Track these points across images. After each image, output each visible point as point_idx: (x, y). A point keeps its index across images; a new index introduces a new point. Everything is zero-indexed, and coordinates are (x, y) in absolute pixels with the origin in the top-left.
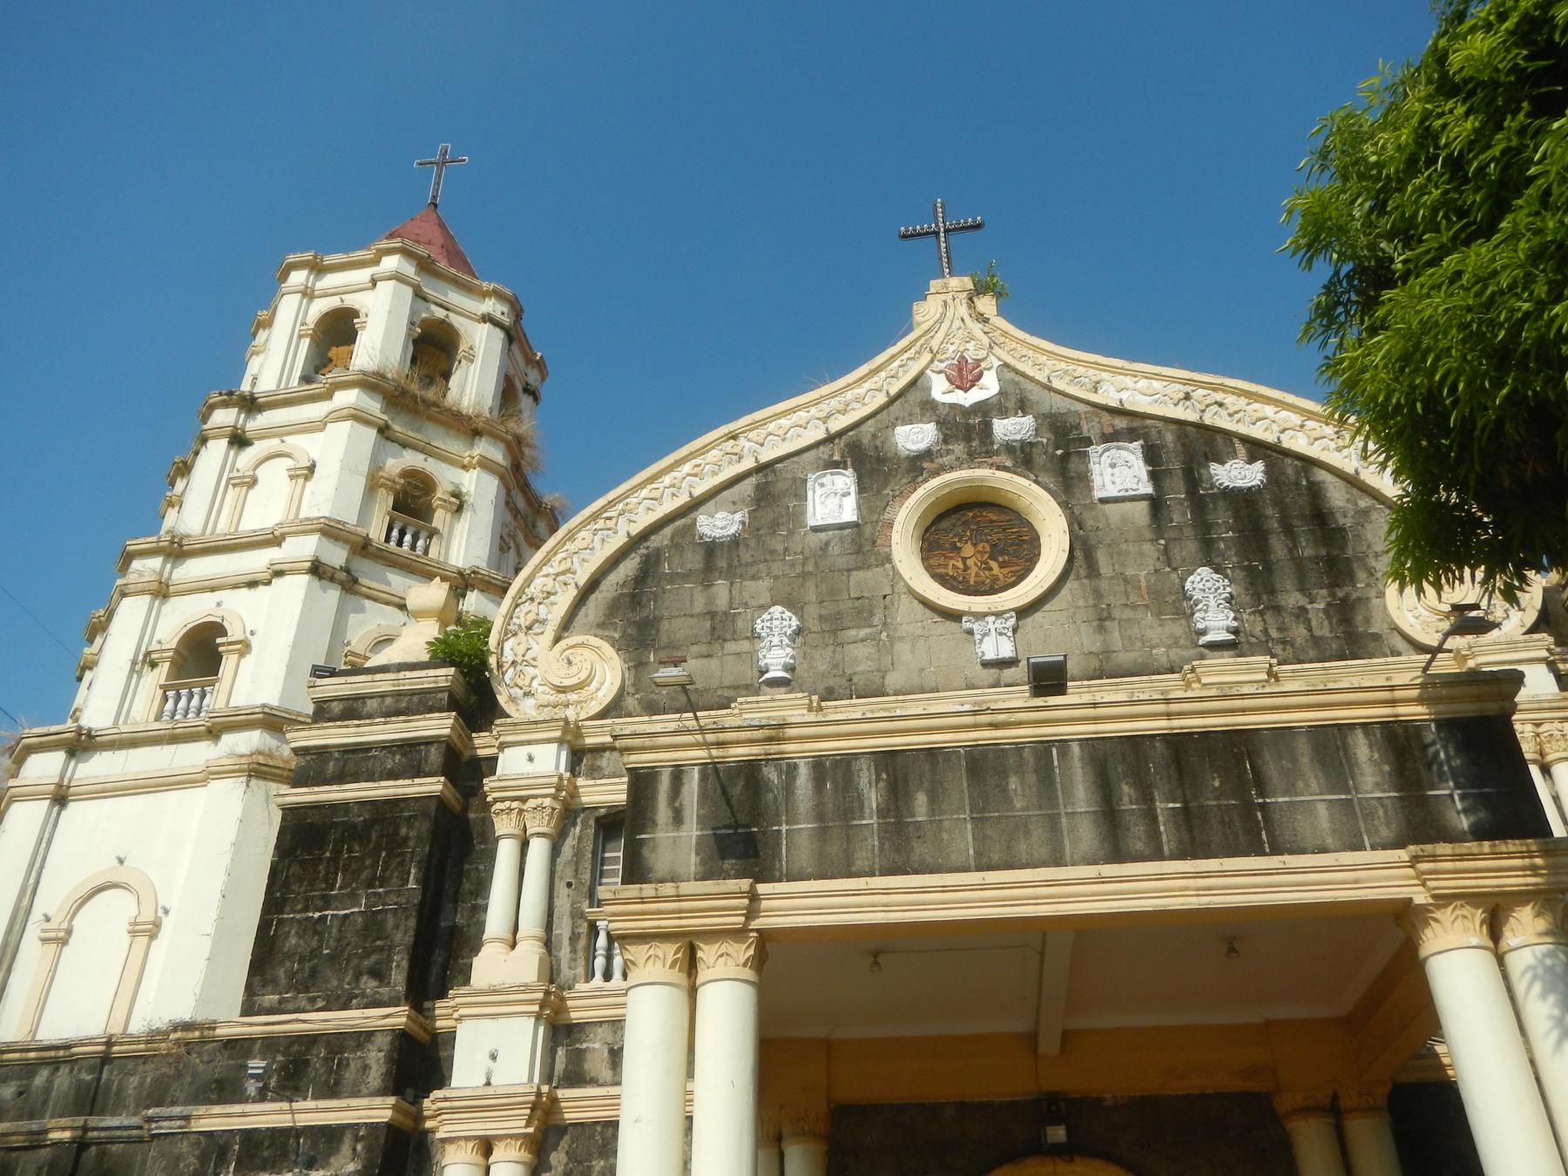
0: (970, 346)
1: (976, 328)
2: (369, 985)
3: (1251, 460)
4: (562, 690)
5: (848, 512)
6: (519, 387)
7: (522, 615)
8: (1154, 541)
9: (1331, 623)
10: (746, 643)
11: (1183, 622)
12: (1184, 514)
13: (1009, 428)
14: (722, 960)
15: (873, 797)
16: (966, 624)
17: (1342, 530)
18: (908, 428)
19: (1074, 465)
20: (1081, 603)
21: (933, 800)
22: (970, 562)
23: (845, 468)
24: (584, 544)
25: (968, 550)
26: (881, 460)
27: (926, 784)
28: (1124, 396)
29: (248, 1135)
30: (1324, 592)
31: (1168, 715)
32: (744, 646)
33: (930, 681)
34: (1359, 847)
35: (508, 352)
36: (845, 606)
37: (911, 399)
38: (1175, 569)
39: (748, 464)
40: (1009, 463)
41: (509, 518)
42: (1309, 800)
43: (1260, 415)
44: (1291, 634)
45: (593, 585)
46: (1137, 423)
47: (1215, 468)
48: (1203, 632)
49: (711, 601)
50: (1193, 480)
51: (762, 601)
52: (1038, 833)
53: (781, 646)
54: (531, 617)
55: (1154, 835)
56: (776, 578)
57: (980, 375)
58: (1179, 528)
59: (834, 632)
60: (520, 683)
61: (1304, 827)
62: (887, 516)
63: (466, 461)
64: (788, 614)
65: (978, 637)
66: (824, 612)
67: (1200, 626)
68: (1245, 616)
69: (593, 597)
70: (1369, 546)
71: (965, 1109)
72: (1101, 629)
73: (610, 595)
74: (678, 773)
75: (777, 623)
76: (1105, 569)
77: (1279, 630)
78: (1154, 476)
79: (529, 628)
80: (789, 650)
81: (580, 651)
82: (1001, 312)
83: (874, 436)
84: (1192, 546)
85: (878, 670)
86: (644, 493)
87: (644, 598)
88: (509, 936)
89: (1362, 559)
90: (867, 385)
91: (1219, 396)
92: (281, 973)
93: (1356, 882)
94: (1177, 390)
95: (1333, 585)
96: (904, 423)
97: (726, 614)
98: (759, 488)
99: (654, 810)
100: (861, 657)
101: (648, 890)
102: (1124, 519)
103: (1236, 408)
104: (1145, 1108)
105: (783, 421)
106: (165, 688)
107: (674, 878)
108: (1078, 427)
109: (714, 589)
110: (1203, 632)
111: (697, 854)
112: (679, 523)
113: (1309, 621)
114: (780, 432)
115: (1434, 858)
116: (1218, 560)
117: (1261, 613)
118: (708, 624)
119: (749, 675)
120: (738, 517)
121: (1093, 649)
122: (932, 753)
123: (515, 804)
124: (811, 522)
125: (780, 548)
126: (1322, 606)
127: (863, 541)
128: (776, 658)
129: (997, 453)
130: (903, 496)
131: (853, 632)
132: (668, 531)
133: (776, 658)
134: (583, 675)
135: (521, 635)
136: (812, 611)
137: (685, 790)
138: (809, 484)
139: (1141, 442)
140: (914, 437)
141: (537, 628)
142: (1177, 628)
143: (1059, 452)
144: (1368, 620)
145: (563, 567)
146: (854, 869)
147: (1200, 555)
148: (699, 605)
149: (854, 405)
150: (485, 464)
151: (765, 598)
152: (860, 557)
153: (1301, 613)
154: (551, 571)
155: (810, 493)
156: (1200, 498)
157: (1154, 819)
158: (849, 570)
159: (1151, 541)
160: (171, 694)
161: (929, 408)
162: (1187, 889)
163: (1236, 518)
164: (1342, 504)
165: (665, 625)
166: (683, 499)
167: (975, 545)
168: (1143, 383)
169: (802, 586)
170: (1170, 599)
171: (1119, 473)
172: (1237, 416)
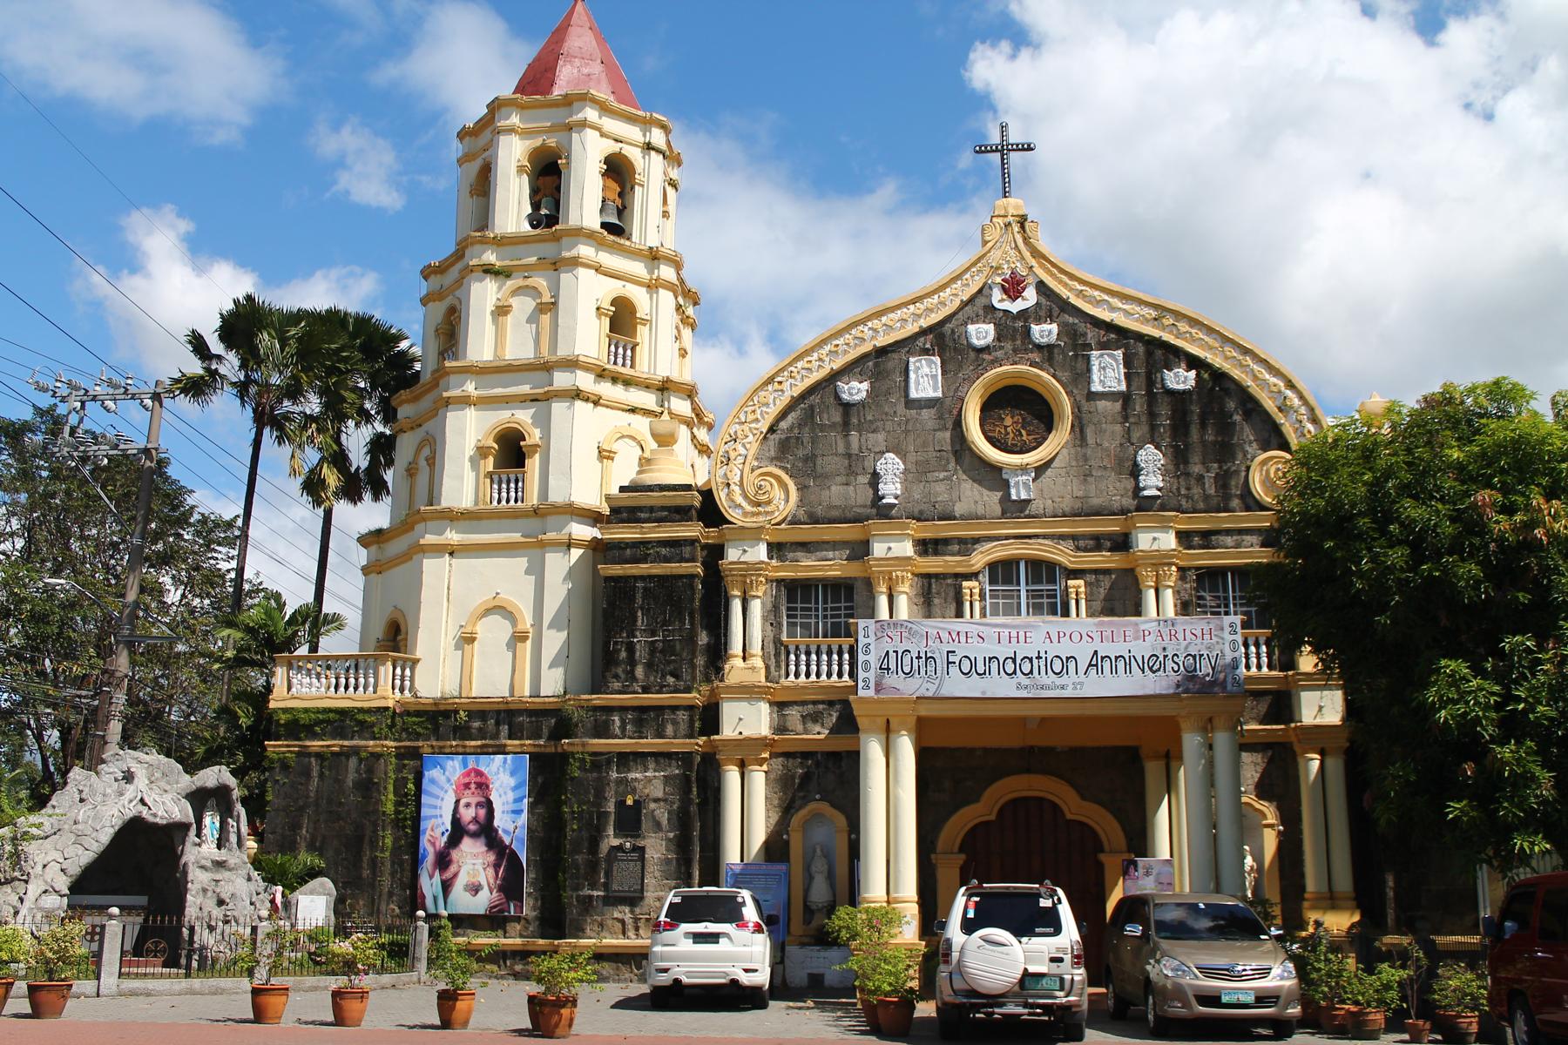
2: (671, 680)
3: (1189, 369)
29: (619, 754)
33: (980, 511)
39: (867, 348)
49: (848, 445)
50: (1150, 383)
71: (985, 749)
75: (891, 468)
76: (1090, 440)
77: (1188, 489)
78: (1127, 376)
84: (1145, 428)
86: (800, 365)
92: (620, 671)
95: (1219, 462)
98: (876, 365)
100: (941, 492)
104: (1074, 752)
105: (891, 315)
106: (490, 475)
127: (948, 412)
136: (912, 457)
138: (912, 367)
140: (981, 333)
148: (841, 449)
153: (1200, 478)
160: (496, 478)
165: (819, 461)
171: (1108, 372)
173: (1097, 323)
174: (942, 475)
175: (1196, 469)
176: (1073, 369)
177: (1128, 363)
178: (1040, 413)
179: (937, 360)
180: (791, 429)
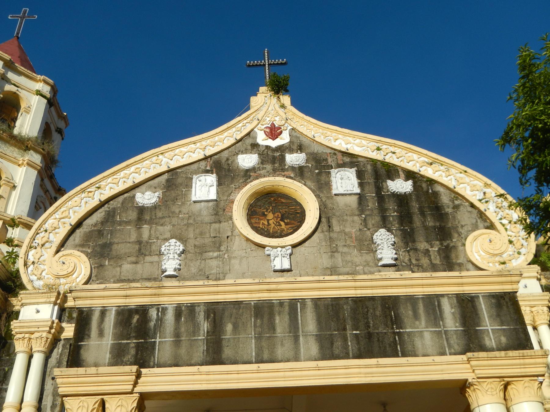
0: (277, 119)
1: (281, 111)
3: (407, 179)
4: (58, 277)
5: (213, 195)
6: (53, 128)
7: (40, 238)
8: (360, 215)
9: (440, 258)
10: (156, 257)
11: (372, 254)
12: (374, 204)
13: (294, 159)
14: (119, 408)
15: (205, 326)
16: (267, 251)
17: (447, 214)
18: (244, 155)
19: (323, 178)
20: (324, 243)
21: (235, 327)
22: (271, 222)
23: (212, 173)
24: (76, 204)
25: (270, 216)
26: (229, 170)
27: (233, 319)
28: (349, 146)
30: (438, 243)
31: (355, 288)
32: (155, 258)
34: (443, 354)
35: (47, 112)
36: (207, 241)
37: (247, 143)
38: (369, 229)
40: (292, 175)
41: (42, 193)
42: (421, 331)
43: (411, 159)
44: (421, 262)
45: (79, 224)
46: (355, 160)
47: (390, 183)
48: (381, 259)
49: (140, 235)
50: (379, 188)
51: (166, 236)
52: (289, 344)
53: (174, 259)
54: (45, 240)
55: (346, 347)
56: (174, 226)
57: (281, 132)
58: (372, 210)
59: (201, 254)
60: (36, 273)
61: (418, 343)
62: (231, 197)
63: (20, 162)
64: (178, 243)
65: (272, 258)
66: (197, 243)
67: (379, 256)
68: (401, 253)
69: (78, 231)
70: (459, 222)
72: (332, 257)
73: (87, 230)
74: (104, 312)
76: (336, 227)
77: (417, 260)
78: (361, 185)
79: (43, 245)
80: (178, 262)
81: (69, 258)
82: (293, 104)
83: (228, 159)
84: (378, 219)
85: (223, 273)
86: (110, 180)
87: (105, 232)
88: (18, 405)
89: (455, 228)
90: (226, 134)
91: (392, 149)
93: (442, 371)
94: (374, 145)
95: (441, 240)
96: (242, 153)
97: (147, 242)
98: (168, 181)
99: (90, 330)
101: (81, 370)
102: (346, 205)
103: (401, 155)
107: (96, 365)
108: (326, 160)
109: (142, 230)
110: (381, 259)
111: (110, 353)
112: (126, 195)
113: (430, 256)
114: (181, 154)
115: (478, 359)
116: (389, 226)
117: (408, 251)
118: (137, 247)
119: (157, 273)
120: (157, 194)
121: (328, 266)
122: (238, 304)
123: (27, 335)
124: (194, 198)
125: (177, 211)
126: (437, 249)
127: (220, 209)
128: (170, 265)
129: (287, 170)
130: (240, 188)
131: (211, 254)
132: (121, 198)
133: (170, 265)
134: (70, 270)
135: (38, 248)
136: (192, 242)
137: (107, 319)
138: (194, 180)
139: (356, 168)
140: (247, 161)
141: (47, 245)
142: (369, 257)
143: (317, 171)
144: (457, 257)
145: (64, 215)
146: (193, 362)
147: (381, 223)
148: (134, 237)
149: (219, 143)
150: (30, 165)
151: (168, 235)
152: (217, 217)
153: (427, 253)
154: (58, 217)
155: (194, 185)
156: (382, 197)
157: (345, 340)
158: (211, 223)
159: (358, 215)
161: (255, 146)
162: (360, 373)
163: (398, 206)
164: (447, 202)
165: (115, 247)
166: (129, 184)
167: (274, 214)
168: (358, 141)
169: (186, 230)
170: (366, 243)
171: (345, 182)
172: (400, 159)
173: (335, 152)
174: (216, 254)
175: (422, 245)
176: (318, 181)
177: (360, 175)
178: (294, 215)
179: (215, 175)
180: (95, 225)
